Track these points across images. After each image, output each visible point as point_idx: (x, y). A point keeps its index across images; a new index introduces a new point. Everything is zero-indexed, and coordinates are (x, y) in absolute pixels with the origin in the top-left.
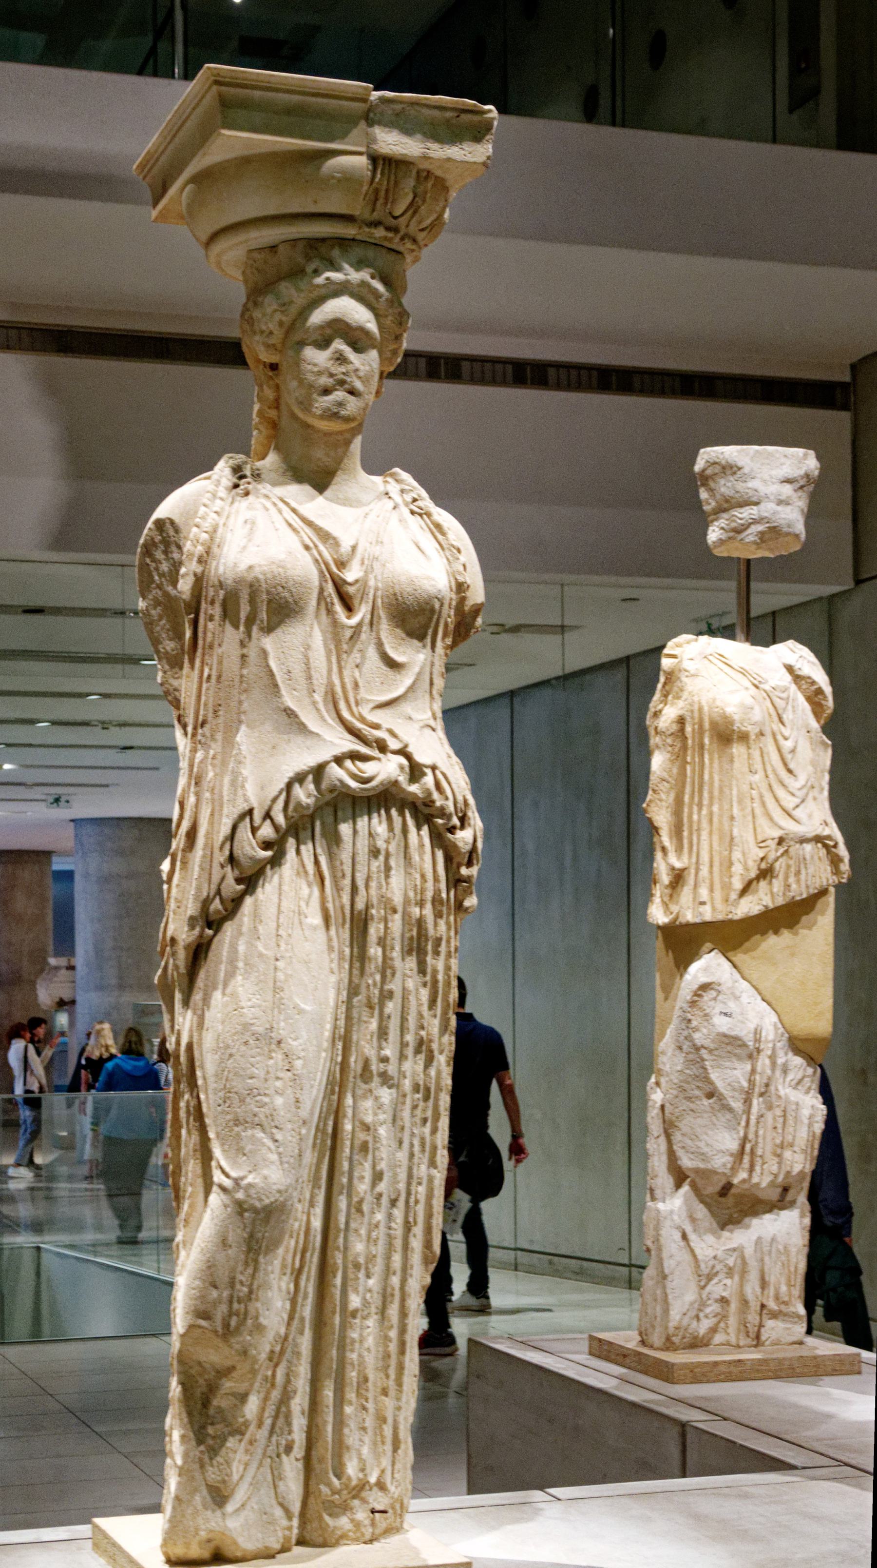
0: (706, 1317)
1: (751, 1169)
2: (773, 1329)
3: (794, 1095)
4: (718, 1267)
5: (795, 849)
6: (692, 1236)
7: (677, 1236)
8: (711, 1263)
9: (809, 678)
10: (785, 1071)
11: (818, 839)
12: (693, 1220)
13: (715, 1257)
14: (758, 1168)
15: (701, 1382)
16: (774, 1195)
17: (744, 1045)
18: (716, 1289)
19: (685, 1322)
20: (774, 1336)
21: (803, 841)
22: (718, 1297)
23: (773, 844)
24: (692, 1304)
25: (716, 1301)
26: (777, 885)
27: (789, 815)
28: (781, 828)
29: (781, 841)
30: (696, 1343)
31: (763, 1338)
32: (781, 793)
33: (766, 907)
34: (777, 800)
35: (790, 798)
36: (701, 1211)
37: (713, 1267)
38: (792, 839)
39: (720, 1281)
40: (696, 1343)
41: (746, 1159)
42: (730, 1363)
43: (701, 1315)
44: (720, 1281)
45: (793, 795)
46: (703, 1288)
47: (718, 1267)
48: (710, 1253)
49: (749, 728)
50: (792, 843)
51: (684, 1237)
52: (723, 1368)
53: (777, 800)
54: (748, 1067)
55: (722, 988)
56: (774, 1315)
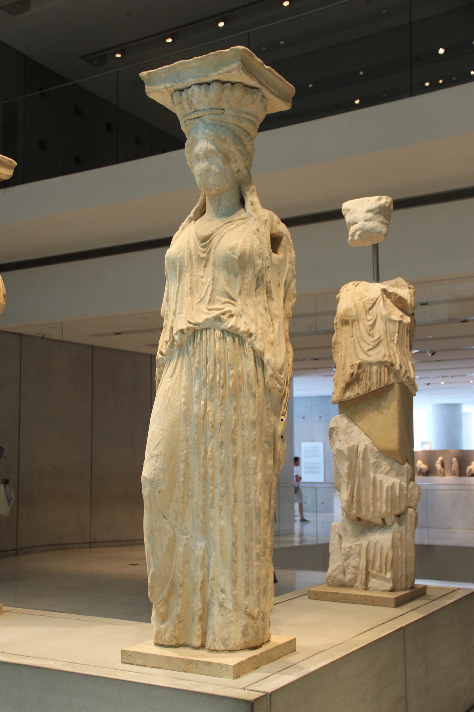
0: (348, 573)
1: (359, 508)
2: (373, 583)
3: (379, 477)
4: (352, 552)
5: (368, 368)
6: (343, 538)
7: (337, 537)
8: (347, 550)
9: (394, 293)
10: (377, 466)
11: (380, 363)
12: (345, 530)
13: (350, 548)
14: (364, 510)
15: (320, 600)
16: (380, 522)
17: (344, 454)
18: (353, 562)
19: (334, 574)
20: (374, 586)
21: (371, 364)
22: (353, 565)
23: (356, 367)
24: (339, 567)
25: (353, 567)
26: (363, 383)
27: (365, 353)
28: (360, 359)
29: (360, 366)
30: (343, 585)
31: (369, 586)
32: (363, 344)
33: (358, 394)
34: (361, 347)
35: (367, 346)
36: (349, 527)
37: (350, 551)
38: (365, 364)
39: (354, 559)
40: (343, 585)
41: (354, 504)
42: (333, 593)
43: (346, 572)
44: (354, 559)
45: (369, 344)
46: (345, 560)
47: (352, 552)
48: (348, 545)
49: (349, 318)
50: (366, 366)
51: (340, 536)
52: (330, 595)
53: (361, 347)
54: (348, 463)
55: (339, 429)
56: (375, 577)
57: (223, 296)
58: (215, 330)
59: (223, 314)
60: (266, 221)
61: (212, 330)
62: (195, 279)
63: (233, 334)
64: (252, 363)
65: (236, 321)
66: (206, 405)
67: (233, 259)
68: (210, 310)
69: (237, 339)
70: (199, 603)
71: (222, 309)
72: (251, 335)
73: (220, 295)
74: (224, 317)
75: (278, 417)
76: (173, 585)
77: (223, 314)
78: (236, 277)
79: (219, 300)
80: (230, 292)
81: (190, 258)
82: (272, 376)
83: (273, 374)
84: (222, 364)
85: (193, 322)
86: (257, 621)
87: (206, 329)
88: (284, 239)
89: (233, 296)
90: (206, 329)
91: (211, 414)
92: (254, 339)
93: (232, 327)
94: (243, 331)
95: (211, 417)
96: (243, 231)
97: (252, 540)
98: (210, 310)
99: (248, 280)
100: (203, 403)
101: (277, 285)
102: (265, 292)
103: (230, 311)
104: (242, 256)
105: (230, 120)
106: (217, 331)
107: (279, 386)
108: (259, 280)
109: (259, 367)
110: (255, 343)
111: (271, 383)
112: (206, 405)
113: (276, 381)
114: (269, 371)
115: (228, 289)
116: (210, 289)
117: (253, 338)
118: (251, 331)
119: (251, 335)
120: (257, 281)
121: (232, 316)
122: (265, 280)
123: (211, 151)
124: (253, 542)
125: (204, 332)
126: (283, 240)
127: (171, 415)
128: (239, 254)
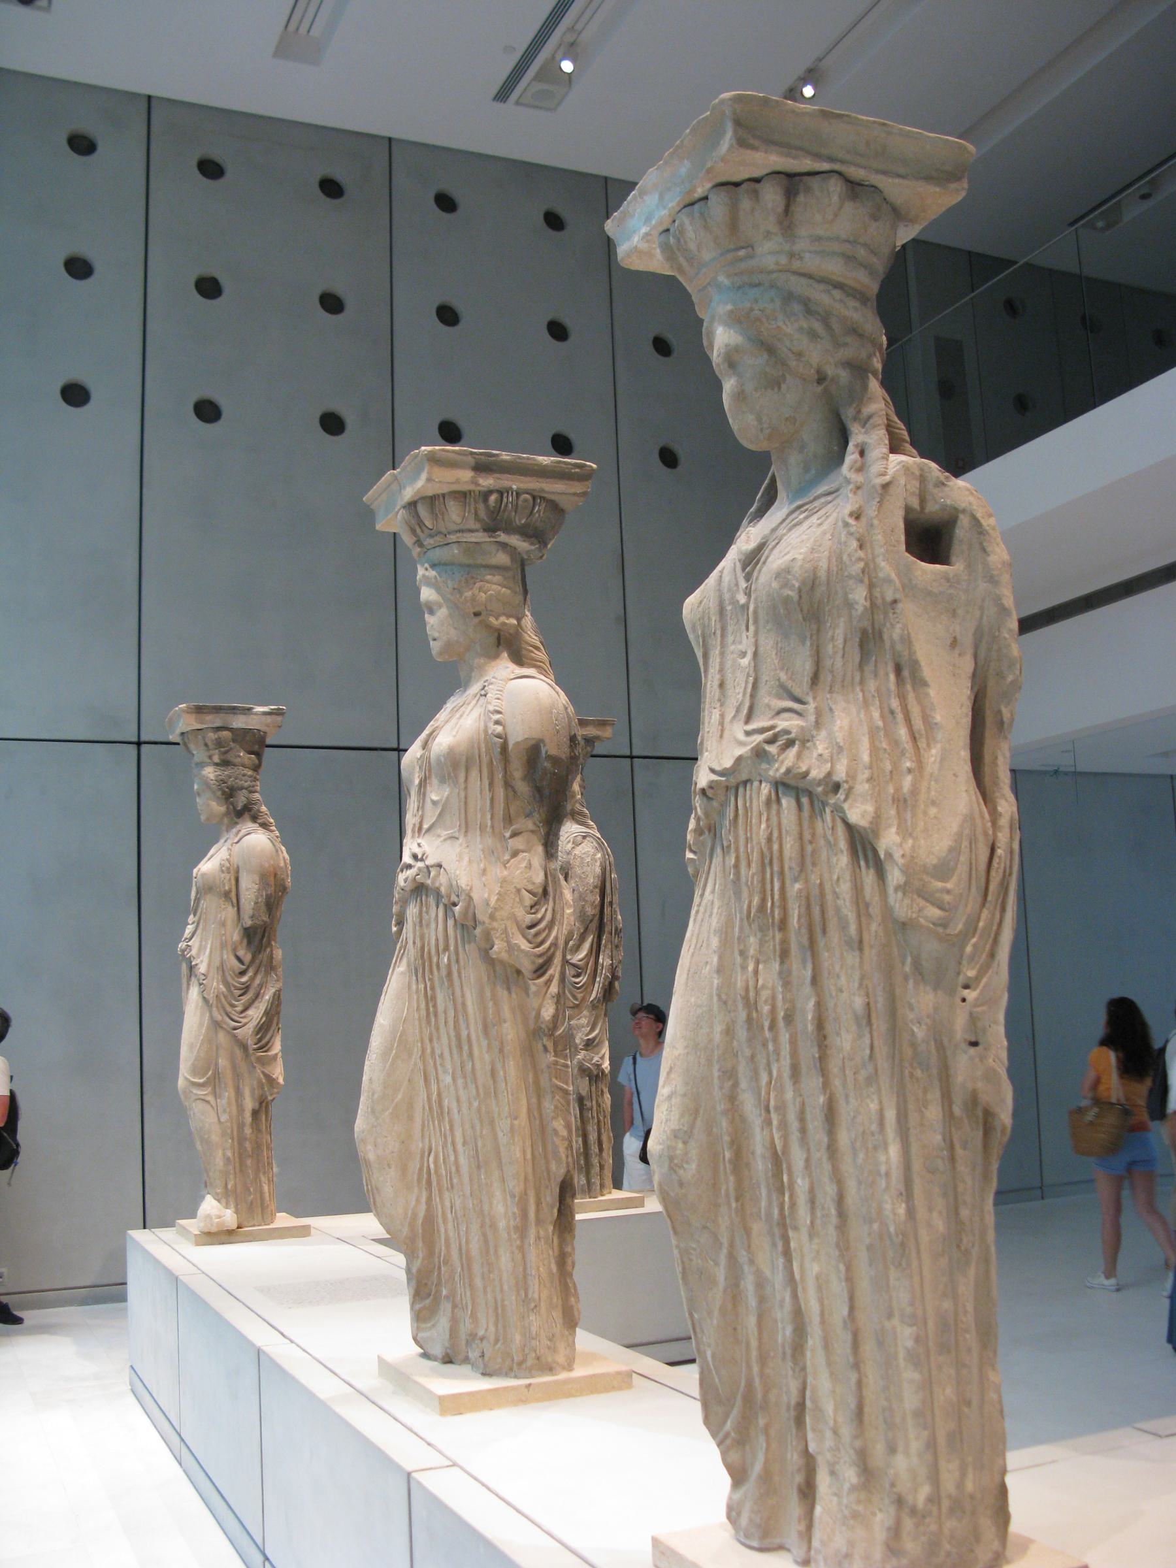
57: (781, 698)
58: (761, 782)
59: (771, 741)
60: (886, 486)
61: (756, 784)
62: (729, 658)
63: (791, 786)
64: (844, 859)
65: (799, 756)
66: (756, 972)
67: (787, 600)
68: (748, 733)
69: (805, 800)
70: (795, 1456)
71: (772, 728)
72: (837, 787)
73: (770, 694)
74: (772, 749)
75: (951, 992)
76: (749, 1398)
77: (771, 741)
78: (804, 644)
79: (768, 706)
80: (789, 684)
81: (722, 611)
82: (903, 888)
83: (905, 884)
84: (776, 868)
85: (718, 768)
86: (927, 1521)
87: (745, 783)
88: (964, 521)
89: (797, 692)
90: (745, 783)
91: (765, 994)
92: (843, 797)
93: (788, 771)
94: (814, 779)
95: (766, 1001)
96: (820, 524)
97: (890, 1316)
98: (748, 733)
99: (834, 646)
100: (751, 968)
101: (949, 642)
102: (890, 668)
103: (787, 732)
104: (811, 584)
105: (770, 262)
106: (763, 785)
107: (934, 912)
108: (869, 640)
109: (868, 867)
110: (846, 806)
111: (901, 906)
112: (756, 972)
113: (922, 903)
114: (895, 876)
115: (783, 676)
116: (751, 679)
117: (841, 795)
118: (836, 778)
119: (837, 787)
120: (862, 645)
121: (790, 743)
122: (885, 637)
123: (737, 349)
124: (896, 1321)
125: (741, 790)
126: (959, 523)
127: (693, 1000)
128: (797, 585)
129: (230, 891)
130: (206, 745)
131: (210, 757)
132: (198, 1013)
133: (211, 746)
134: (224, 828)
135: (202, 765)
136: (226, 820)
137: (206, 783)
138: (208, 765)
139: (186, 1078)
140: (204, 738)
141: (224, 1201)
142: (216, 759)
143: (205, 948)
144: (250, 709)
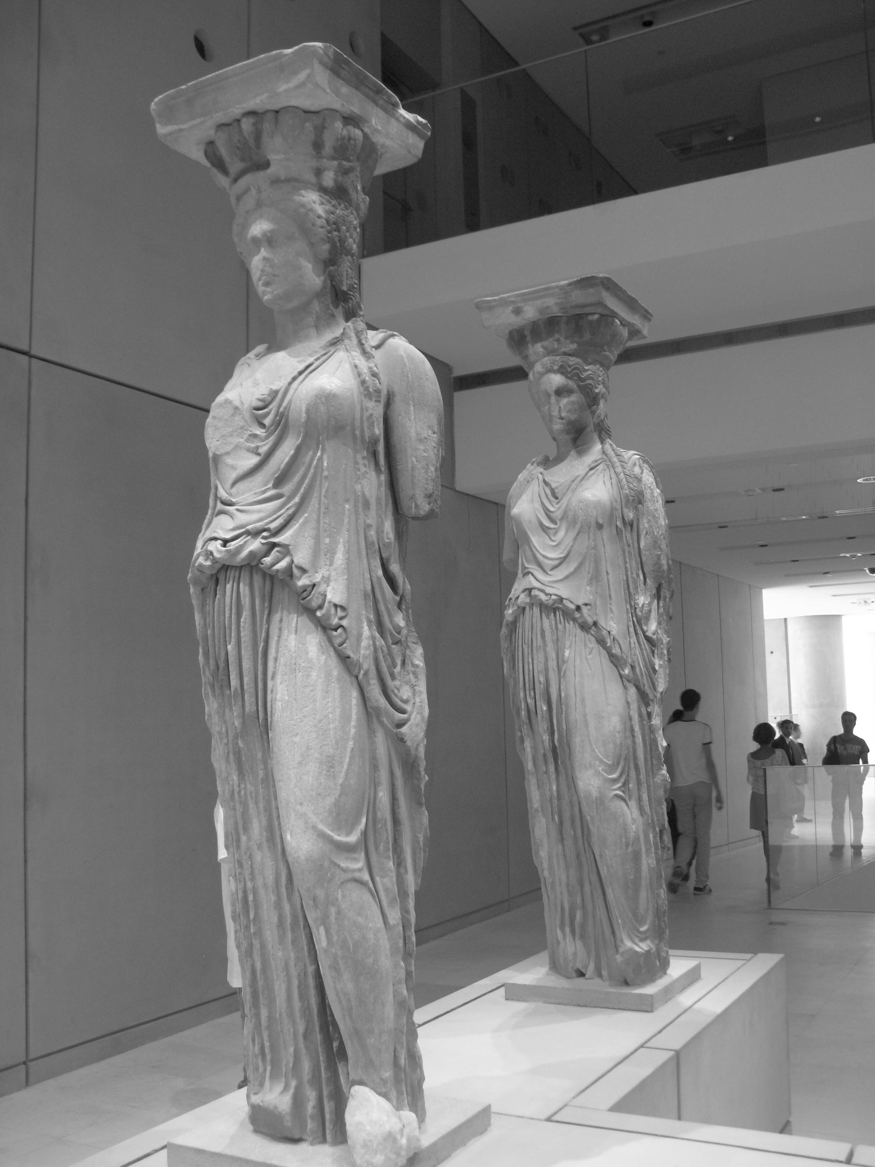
129: (375, 442)
130: (318, 146)
131: (318, 172)
132: (335, 687)
133: (328, 149)
134: (311, 320)
135: (294, 182)
136: (316, 306)
137: (302, 222)
138: (307, 185)
139: (322, 836)
140: (320, 130)
141: (393, 1094)
142: (329, 179)
143: (332, 552)
144: (395, 105)
